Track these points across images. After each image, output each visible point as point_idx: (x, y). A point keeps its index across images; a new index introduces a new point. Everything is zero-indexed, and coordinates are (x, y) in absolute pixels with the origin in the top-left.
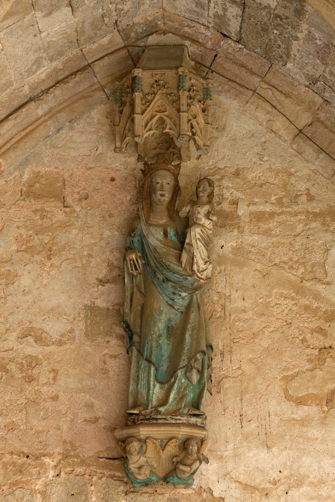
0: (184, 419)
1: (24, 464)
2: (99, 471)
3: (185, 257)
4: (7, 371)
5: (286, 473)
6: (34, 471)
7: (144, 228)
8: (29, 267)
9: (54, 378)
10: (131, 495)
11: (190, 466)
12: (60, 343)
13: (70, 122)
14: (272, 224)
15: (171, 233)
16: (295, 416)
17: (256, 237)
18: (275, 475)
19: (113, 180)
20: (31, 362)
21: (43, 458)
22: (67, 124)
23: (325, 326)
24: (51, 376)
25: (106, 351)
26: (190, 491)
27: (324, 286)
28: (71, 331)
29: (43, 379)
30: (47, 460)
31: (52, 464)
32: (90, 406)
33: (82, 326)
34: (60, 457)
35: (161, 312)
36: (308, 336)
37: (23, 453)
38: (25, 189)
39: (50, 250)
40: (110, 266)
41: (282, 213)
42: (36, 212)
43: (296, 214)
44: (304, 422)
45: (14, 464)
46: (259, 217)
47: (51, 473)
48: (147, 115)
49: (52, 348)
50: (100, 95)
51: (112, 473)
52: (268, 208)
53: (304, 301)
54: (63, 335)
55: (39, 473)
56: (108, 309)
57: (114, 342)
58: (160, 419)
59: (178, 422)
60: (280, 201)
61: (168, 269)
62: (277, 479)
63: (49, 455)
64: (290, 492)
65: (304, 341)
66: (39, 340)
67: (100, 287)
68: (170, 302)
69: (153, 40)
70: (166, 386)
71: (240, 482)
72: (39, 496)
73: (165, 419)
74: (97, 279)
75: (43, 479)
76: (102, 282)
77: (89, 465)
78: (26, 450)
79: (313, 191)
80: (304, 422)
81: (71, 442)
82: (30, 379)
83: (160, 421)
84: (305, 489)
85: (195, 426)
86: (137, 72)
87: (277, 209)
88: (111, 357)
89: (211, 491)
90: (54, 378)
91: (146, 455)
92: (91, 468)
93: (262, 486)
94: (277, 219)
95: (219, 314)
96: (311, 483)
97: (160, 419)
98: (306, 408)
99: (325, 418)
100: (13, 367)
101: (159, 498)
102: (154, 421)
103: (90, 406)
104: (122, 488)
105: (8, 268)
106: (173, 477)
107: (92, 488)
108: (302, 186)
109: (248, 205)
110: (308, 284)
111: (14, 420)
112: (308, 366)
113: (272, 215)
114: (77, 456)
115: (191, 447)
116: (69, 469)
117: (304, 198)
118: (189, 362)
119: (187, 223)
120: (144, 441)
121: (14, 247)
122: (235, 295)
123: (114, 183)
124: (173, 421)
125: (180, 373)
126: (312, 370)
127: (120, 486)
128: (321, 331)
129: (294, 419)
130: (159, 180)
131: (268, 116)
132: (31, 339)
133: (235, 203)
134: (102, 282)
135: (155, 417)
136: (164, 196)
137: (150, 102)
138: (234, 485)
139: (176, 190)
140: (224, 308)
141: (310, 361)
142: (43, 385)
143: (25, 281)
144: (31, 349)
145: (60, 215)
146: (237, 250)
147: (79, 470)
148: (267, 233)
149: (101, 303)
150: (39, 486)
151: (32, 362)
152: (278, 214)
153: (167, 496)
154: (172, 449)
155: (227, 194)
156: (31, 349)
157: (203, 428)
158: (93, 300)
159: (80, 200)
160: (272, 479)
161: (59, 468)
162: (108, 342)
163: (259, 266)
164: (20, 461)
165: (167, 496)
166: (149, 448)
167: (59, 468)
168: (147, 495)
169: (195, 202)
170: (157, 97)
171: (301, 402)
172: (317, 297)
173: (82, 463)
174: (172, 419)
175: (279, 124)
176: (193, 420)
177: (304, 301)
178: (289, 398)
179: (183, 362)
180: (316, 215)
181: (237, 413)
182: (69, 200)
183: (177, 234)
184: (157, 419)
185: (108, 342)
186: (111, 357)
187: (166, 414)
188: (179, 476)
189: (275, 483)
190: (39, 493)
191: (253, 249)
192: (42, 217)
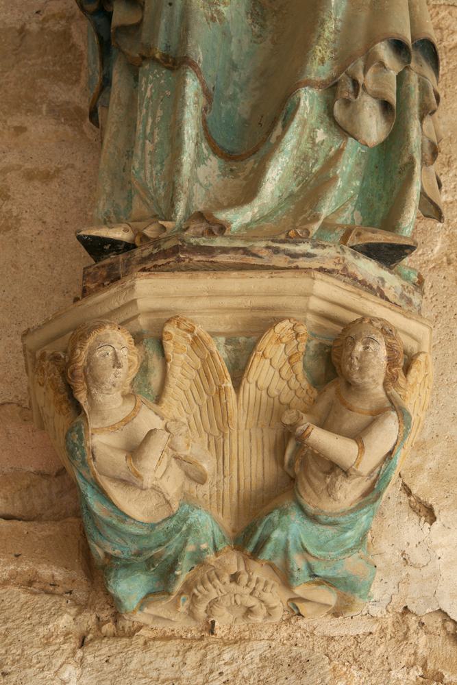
11: (358, 436)
51: (25, 567)
56: (22, 32)
58: (225, 250)
59: (302, 263)
73: (246, 251)
83: (221, 258)
91: (163, 409)
97: (225, 250)
101: (227, 657)
102: (197, 258)
104: (65, 621)
106: (284, 512)
115: (359, 348)
118: (343, 69)
124: (280, 261)
125: (308, 102)
127: (59, 613)
135: (203, 242)
153: (258, 648)
165: (258, 648)
166: (176, 371)
168: (173, 646)
174: (276, 251)
176: (368, 268)
179: (320, 67)
184: (210, 251)
185: (20, 130)
186: (30, 176)
187: (250, 231)
188: (310, 509)
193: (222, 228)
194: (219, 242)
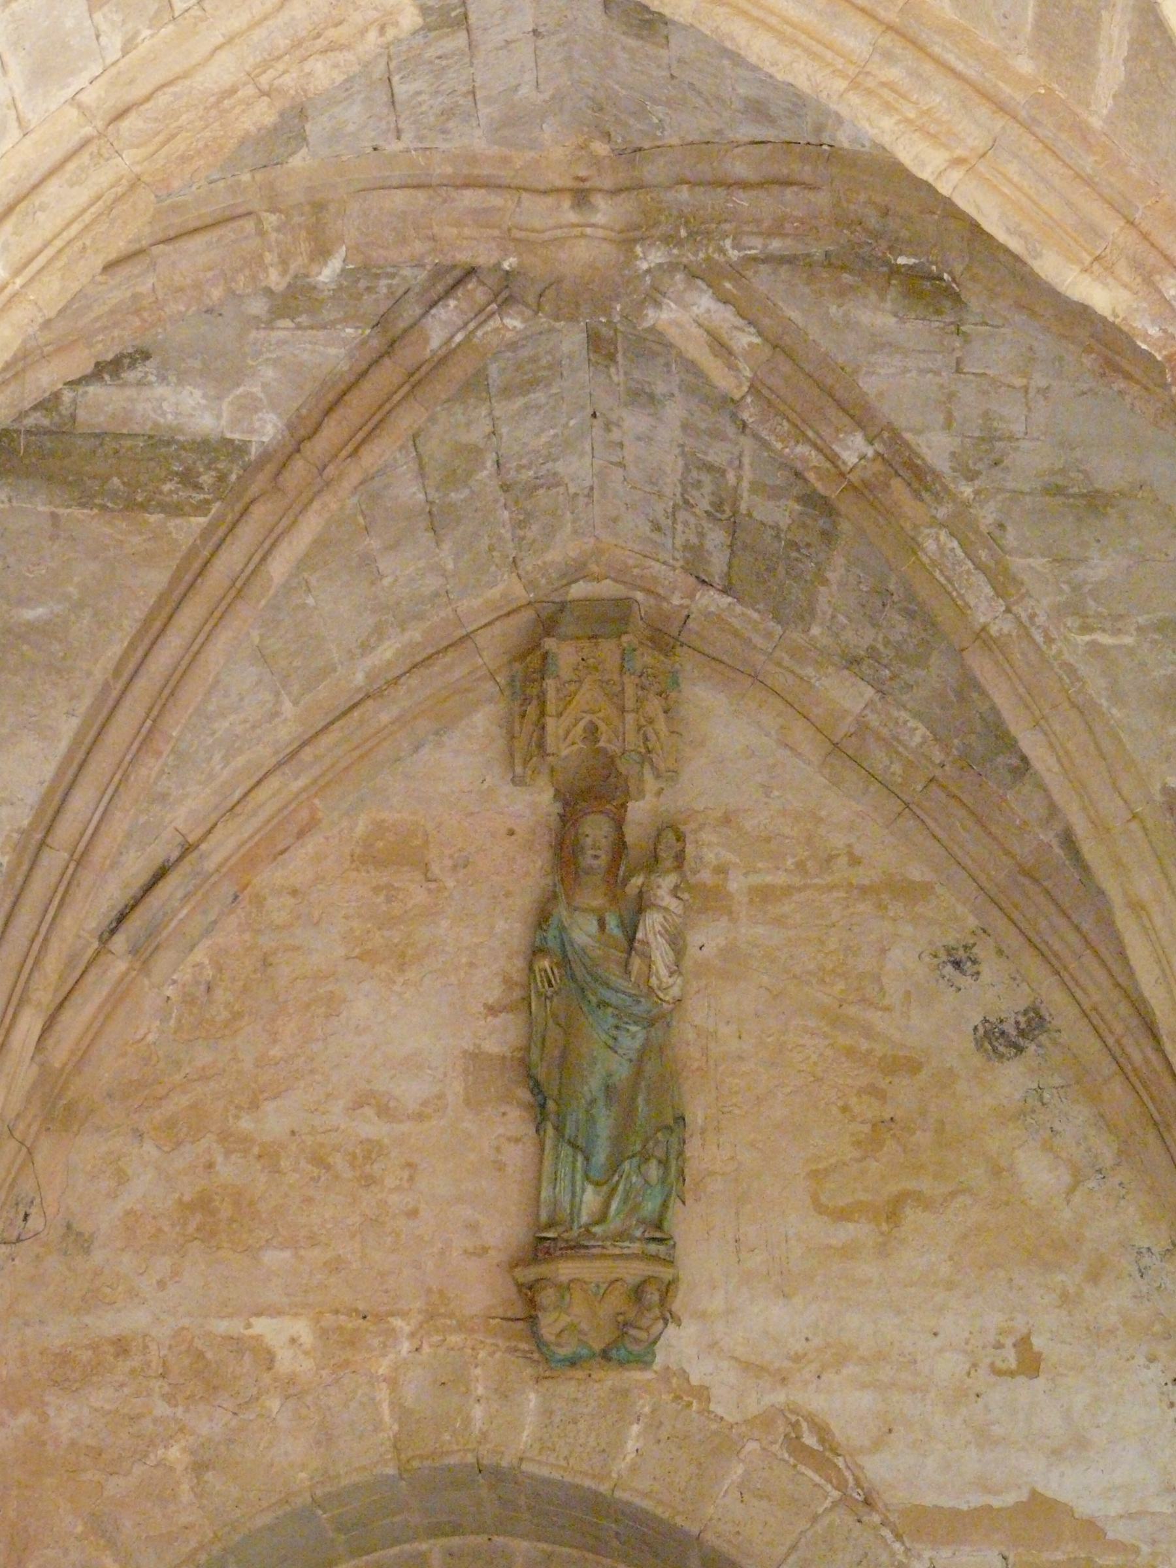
0: (636, 1247)
1: (358, 1329)
2: (489, 1341)
3: (636, 963)
4: (328, 1168)
5: (817, 1341)
6: (376, 1342)
7: (565, 913)
8: (366, 986)
9: (411, 1179)
10: (547, 1383)
12: (420, 1117)
13: (437, 733)
14: (786, 908)
15: (612, 922)
16: (834, 1242)
17: (760, 930)
18: (797, 1346)
19: (511, 833)
20: (370, 1152)
21: (391, 1319)
22: (431, 737)
23: (883, 1084)
24: (406, 1174)
25: (501, 1130)
26: (648, 1375)
27: (880, 1013)
28: (440, 1096)
29: (390, 1182)
30: (397, 1322)
31: (407, 1329)
32: (473, 1227)
33: (458, 1087)
34: (421, 1317)
35: (594, 1060)
36: (853, 1101)
37: (356, 1310)
38: (358, 851)
39: (403, 955)
40: (508, 982)
41: (806, 887)
42: (377, 890)
43: (831, 888)
44: (848, 1252)
45: (340, 1329)
46: (764, 895)
47: (406, 1346)
48: (566, 721)
49: (406, 1127)
50: (489, 687)
51: (513, 1344)
52: (781, 879)
53: (844, 1040)
54: (425, 1103)
55: (385, 1346)
56: (504, 1057)
57: (515, 1113)
58: (594, 1247)
59: (626, 1251)
60: (801, 866)
61: (606, 984)
62: (801, 1352)
63: (403, 1314)
64: (824, 1377)
65: (845, 1109)
66: (385, 1111)
67: (490, 1018)
68: (611, 1042)
69: (578, 590)
70: (605, 1189)
71: (736, 1359)
72: (384, 1386)
73: (603, 1247)
74: (485, 1005)
75: (392, 1356)
76: (492, 1010)
77: (472, 1331)
78: (361, 1306)
79: (858, 849)
80: (848, 1252)
81: (441, 1292)
82: (369, 1181)
83: (595, 1251)
84: (850, 1369)
85: (655, 1258)
86: (549, 644)
87: (797, 881)
88: (509, 1139)
89: (684, 1375)
90: (411, 1179)
92: (476, 1336)
93: (777, 1365)
94: (796, 897)
95: (696, 1065)
96: (862, 1358)
97: (594, 1247)
98: (850, 1226)
99: (885, 1244)
100: (338, 1161)
103: (473, 1227)
105: (330, 987)
107: (478, 1371)
108: (838, 841)
109: (746, 875)
110: (852, 1010)
111: (341, 1252)
112: (857, 1154)
113: (788, 890)
114: (451, 1316)
116: (436, 1338)
117: (843, 860)
119: (641, 905)
120: (564, 1289)
121: (341, 951)
122: (724, 1030)
123: (513, 838)
124: (617, 1251)
126: (864, 1158)
128: (880, 1095)
129: (829, 1247)
130: (588, 831)
131: (780, 720)
132: (369, 1111)
133: (721, 870)
134: (492, 1010)
135: (586, 1243)
136: (595, 856)
137: (572, 695)
138: (725, 1364)
139: (620, 847)
140: (705, 1051)
141: (858, 1144)
142: (391, 1191)
143: (361, 1008)
144: (371, 1127)
145: (419, 896)
146: (729, 952)
147: (454, 1339)
148: (779, 921)
149: (492, 1046)
150: (383, 1367)
151: (372, 1150)
152: (800, 890)
154: (616, 1301)
155: (710, 856)
156: (371, 1127)
157: (670, 1262)
158: (477, 1041)
159: (455, 868)
160: (792, 1353)
161: (419, 1336)
162: (504, 1114)
163: (765, 979)
164: (350, 1325)
167: (419, 1336)
169: (652, 863)
170: (586, 686)
171: (842, 1215)
172: (868, 1032)
173: (460, 1327)
175: (800, 733)
176: (653, 1248)
177: (844, 1040)
178: (820, 1208)
180: (864, 890)
181: (730, 1236)
182: (435, 869)
183: (622, 925)
184: (586, 1247)
185: (504, 1114)
186: (509, 1139)
189: (797, 1358)
190: (384, 1380)
191: (755, 951)
192: (389, 900)
193: (594, 1235)
194: (592, 1243)
